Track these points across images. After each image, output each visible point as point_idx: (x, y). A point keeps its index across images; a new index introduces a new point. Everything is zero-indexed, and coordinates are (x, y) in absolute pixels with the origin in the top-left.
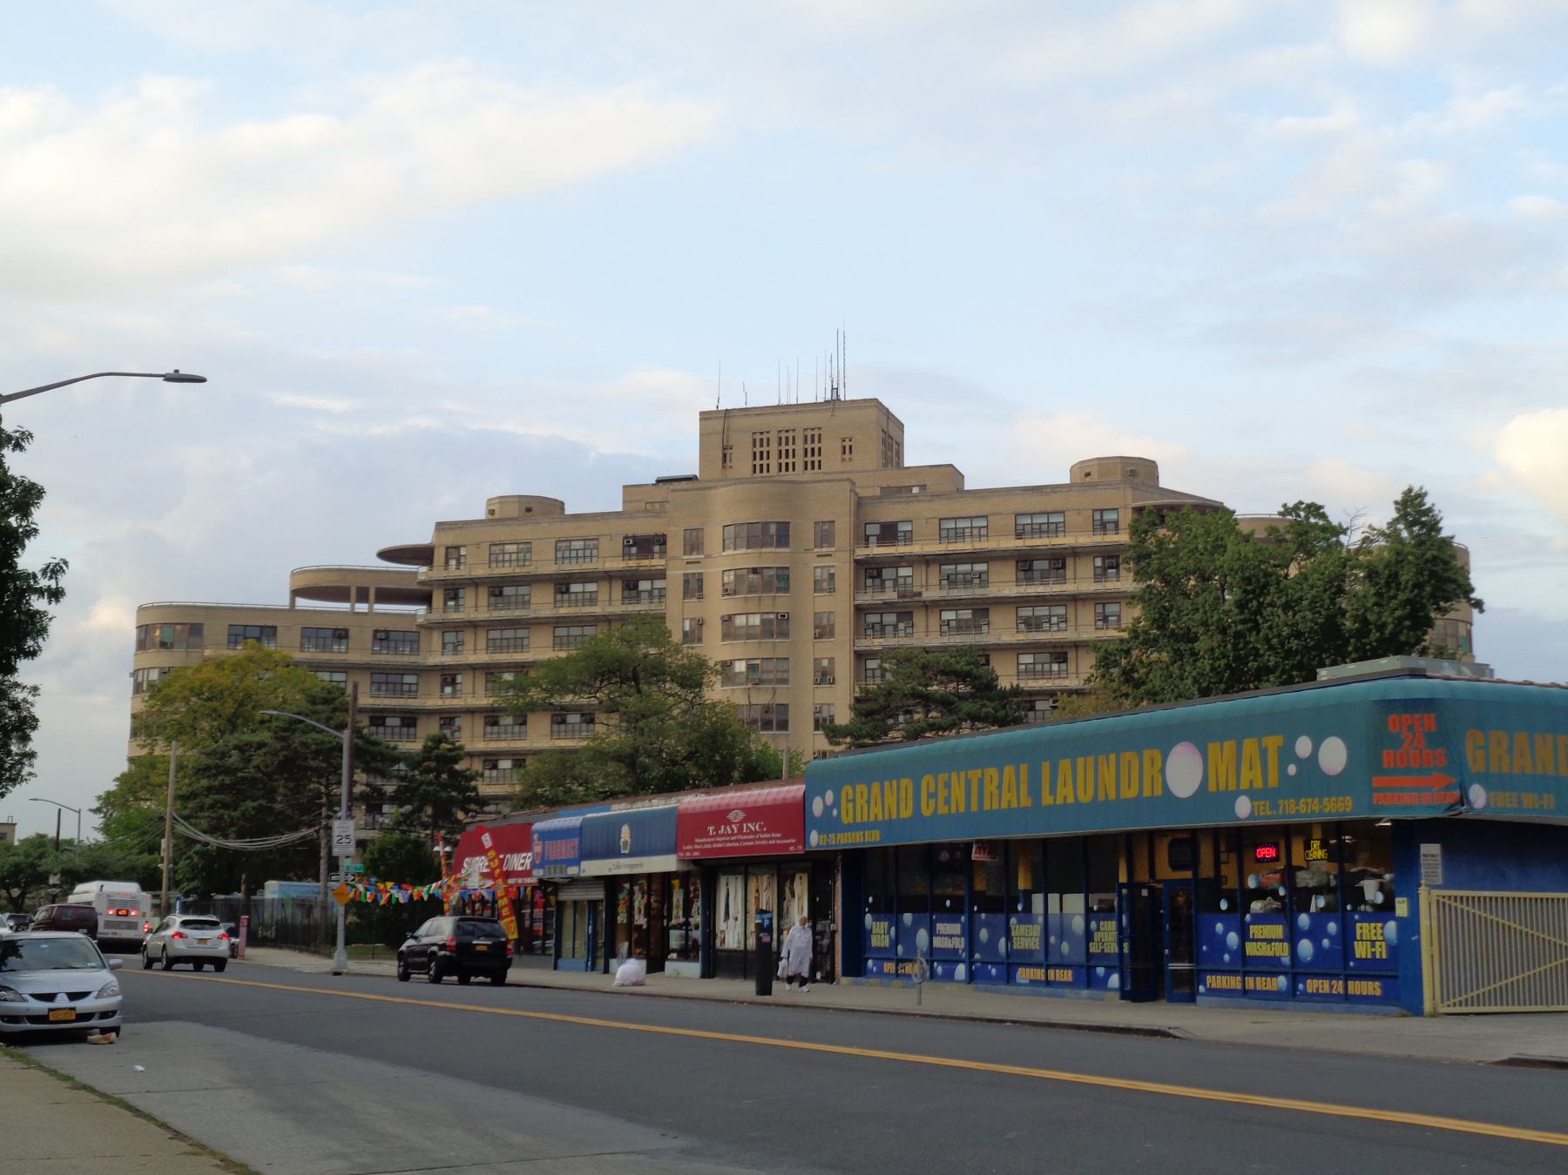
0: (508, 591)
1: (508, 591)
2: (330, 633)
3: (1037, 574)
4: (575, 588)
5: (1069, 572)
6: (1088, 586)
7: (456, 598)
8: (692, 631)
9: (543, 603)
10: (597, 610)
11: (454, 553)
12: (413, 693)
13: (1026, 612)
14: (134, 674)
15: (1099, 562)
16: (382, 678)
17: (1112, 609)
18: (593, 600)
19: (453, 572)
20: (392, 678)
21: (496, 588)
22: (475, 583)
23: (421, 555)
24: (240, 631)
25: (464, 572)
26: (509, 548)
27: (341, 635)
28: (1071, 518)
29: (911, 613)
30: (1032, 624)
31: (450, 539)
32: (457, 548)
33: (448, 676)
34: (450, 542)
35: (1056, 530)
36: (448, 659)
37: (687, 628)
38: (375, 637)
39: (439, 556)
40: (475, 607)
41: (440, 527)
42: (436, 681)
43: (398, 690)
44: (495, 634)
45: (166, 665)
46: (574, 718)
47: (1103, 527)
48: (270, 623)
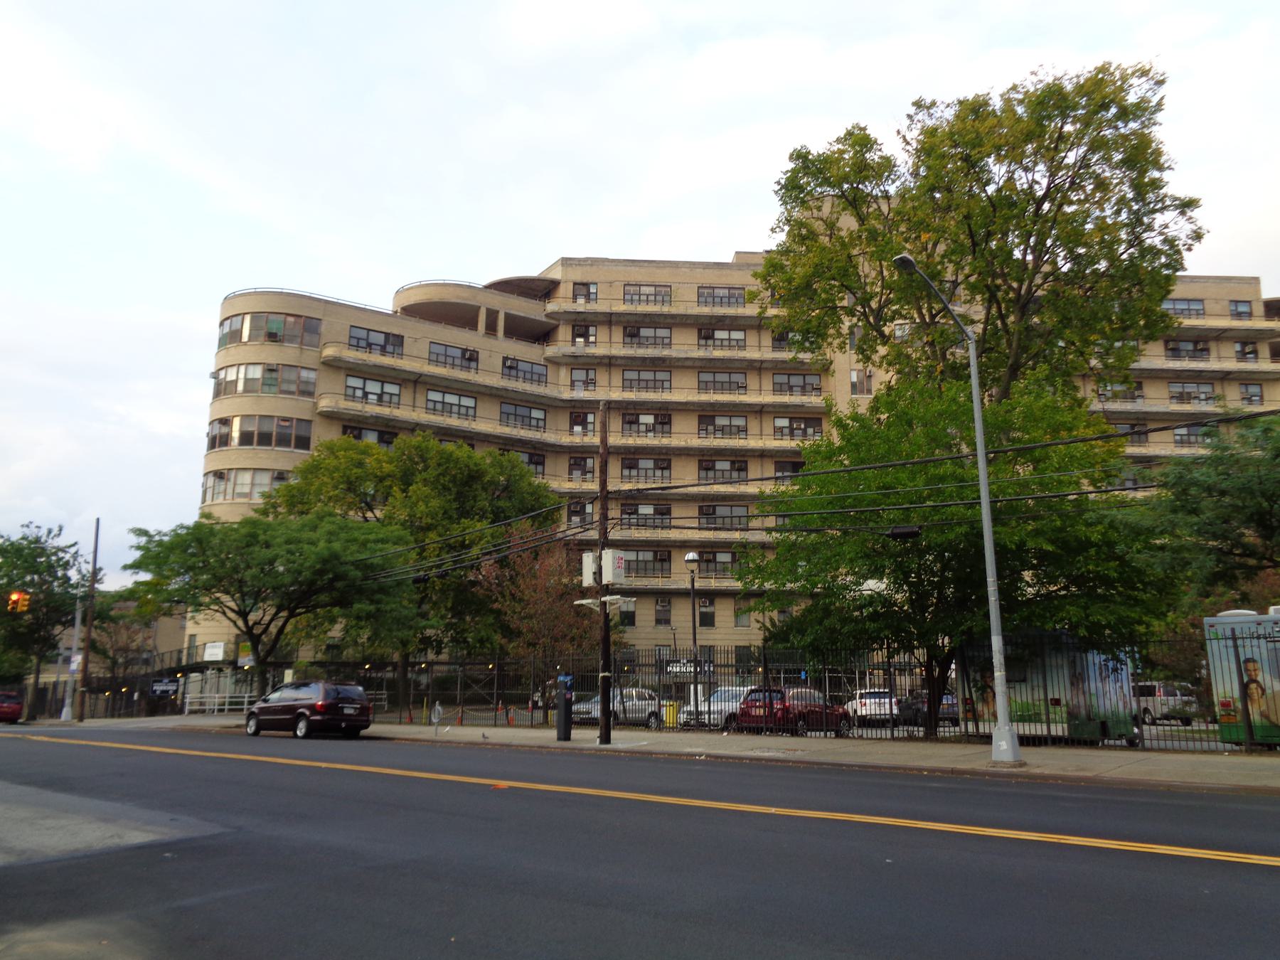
0: (645, 332)
1: (645, 332)
2: (458, 353)
3: (1183, 353)
4: (720, 334)
5: (1213, 354)
6: (1232, 365)
7: (585, 335)
8: (861, 383)
9: (685, 345)
10: (752, 354)
11: (584, 291)
12: (541, 426)
13: (1177, 388)
14: (215, 375)
15: (1238, 347)
16: (511, 409)
17: (1254, 389)
18: (742, 345)
19: (581, 305)
20: (521, 411)
21: (632, 327)
22: (609, 320)
23: (541, 289)
24: (363, 334)
25: (601, 307)
26: (645, 290)
27: (470, 358)
28: (1209, 306)
29: (820, 419)
30: (1182, 398)
31: (578, 275)
32: (586, 285)
33: (578, 413)
34: (579, 279)
35: (1201, 314)
36: (581, 394)
37: (854, 379)
38: (504, 364)
39: (565, 290)
40: (606, 344)
41: (566, 262)
42: (564, 421)
43: (527, 422)
44: (632, 375)
45: (273, 360)
46: (723, 465)
47: (1238, 315)
48: (396, 332)
